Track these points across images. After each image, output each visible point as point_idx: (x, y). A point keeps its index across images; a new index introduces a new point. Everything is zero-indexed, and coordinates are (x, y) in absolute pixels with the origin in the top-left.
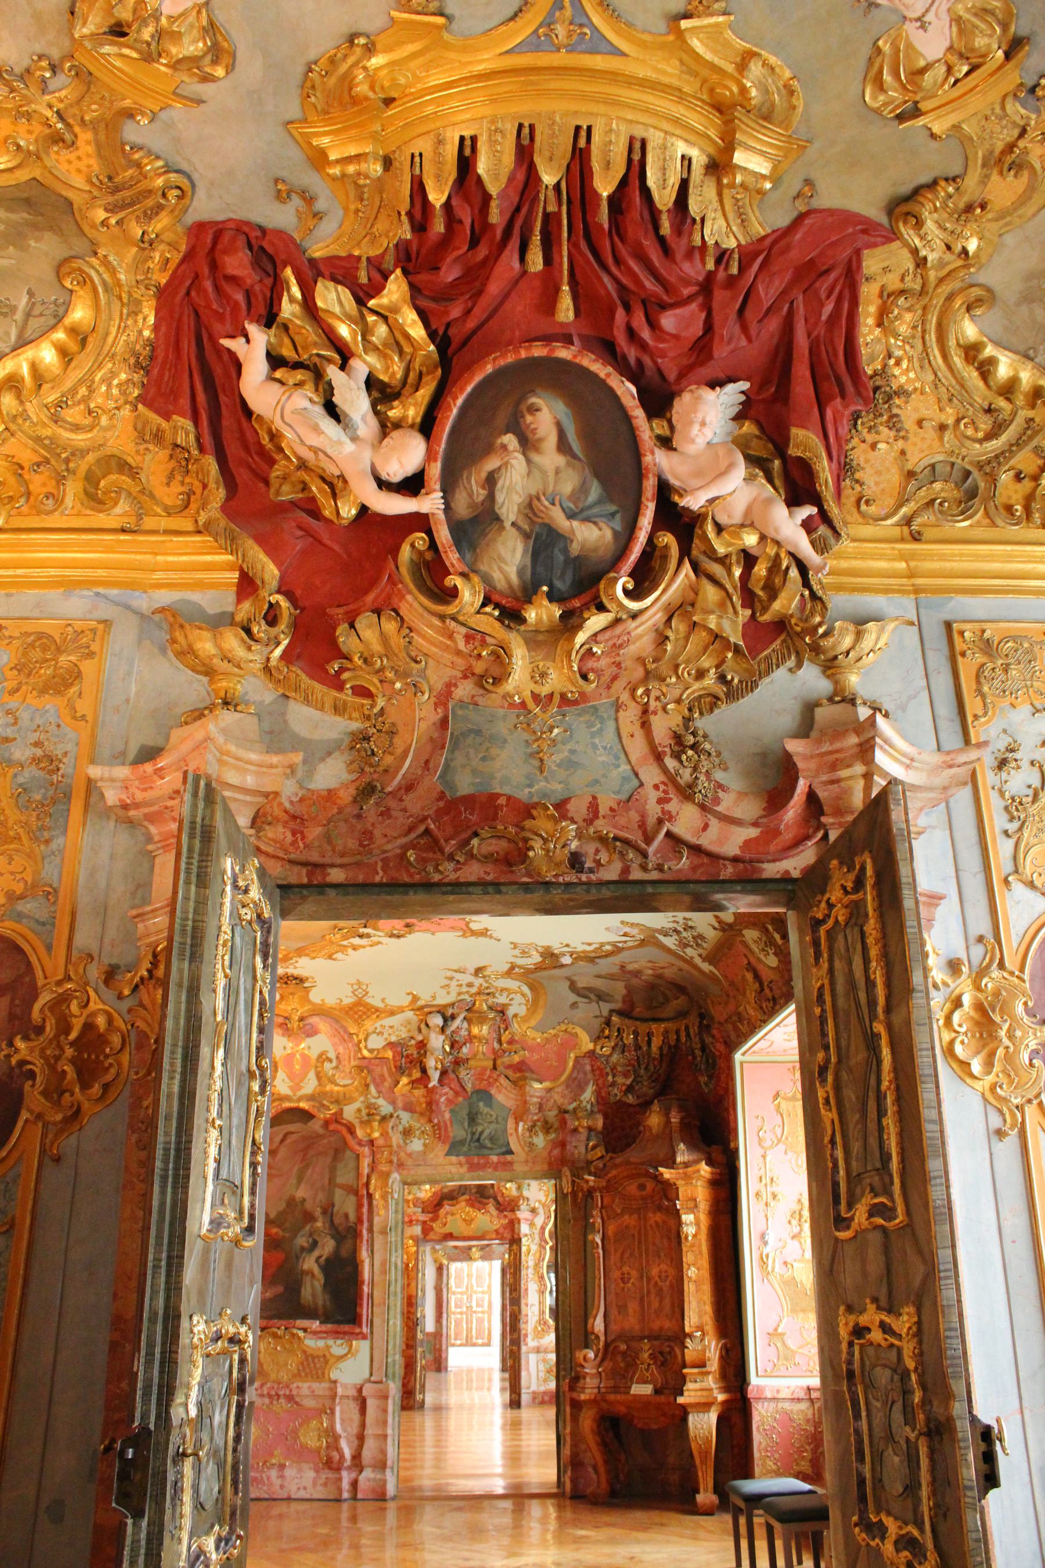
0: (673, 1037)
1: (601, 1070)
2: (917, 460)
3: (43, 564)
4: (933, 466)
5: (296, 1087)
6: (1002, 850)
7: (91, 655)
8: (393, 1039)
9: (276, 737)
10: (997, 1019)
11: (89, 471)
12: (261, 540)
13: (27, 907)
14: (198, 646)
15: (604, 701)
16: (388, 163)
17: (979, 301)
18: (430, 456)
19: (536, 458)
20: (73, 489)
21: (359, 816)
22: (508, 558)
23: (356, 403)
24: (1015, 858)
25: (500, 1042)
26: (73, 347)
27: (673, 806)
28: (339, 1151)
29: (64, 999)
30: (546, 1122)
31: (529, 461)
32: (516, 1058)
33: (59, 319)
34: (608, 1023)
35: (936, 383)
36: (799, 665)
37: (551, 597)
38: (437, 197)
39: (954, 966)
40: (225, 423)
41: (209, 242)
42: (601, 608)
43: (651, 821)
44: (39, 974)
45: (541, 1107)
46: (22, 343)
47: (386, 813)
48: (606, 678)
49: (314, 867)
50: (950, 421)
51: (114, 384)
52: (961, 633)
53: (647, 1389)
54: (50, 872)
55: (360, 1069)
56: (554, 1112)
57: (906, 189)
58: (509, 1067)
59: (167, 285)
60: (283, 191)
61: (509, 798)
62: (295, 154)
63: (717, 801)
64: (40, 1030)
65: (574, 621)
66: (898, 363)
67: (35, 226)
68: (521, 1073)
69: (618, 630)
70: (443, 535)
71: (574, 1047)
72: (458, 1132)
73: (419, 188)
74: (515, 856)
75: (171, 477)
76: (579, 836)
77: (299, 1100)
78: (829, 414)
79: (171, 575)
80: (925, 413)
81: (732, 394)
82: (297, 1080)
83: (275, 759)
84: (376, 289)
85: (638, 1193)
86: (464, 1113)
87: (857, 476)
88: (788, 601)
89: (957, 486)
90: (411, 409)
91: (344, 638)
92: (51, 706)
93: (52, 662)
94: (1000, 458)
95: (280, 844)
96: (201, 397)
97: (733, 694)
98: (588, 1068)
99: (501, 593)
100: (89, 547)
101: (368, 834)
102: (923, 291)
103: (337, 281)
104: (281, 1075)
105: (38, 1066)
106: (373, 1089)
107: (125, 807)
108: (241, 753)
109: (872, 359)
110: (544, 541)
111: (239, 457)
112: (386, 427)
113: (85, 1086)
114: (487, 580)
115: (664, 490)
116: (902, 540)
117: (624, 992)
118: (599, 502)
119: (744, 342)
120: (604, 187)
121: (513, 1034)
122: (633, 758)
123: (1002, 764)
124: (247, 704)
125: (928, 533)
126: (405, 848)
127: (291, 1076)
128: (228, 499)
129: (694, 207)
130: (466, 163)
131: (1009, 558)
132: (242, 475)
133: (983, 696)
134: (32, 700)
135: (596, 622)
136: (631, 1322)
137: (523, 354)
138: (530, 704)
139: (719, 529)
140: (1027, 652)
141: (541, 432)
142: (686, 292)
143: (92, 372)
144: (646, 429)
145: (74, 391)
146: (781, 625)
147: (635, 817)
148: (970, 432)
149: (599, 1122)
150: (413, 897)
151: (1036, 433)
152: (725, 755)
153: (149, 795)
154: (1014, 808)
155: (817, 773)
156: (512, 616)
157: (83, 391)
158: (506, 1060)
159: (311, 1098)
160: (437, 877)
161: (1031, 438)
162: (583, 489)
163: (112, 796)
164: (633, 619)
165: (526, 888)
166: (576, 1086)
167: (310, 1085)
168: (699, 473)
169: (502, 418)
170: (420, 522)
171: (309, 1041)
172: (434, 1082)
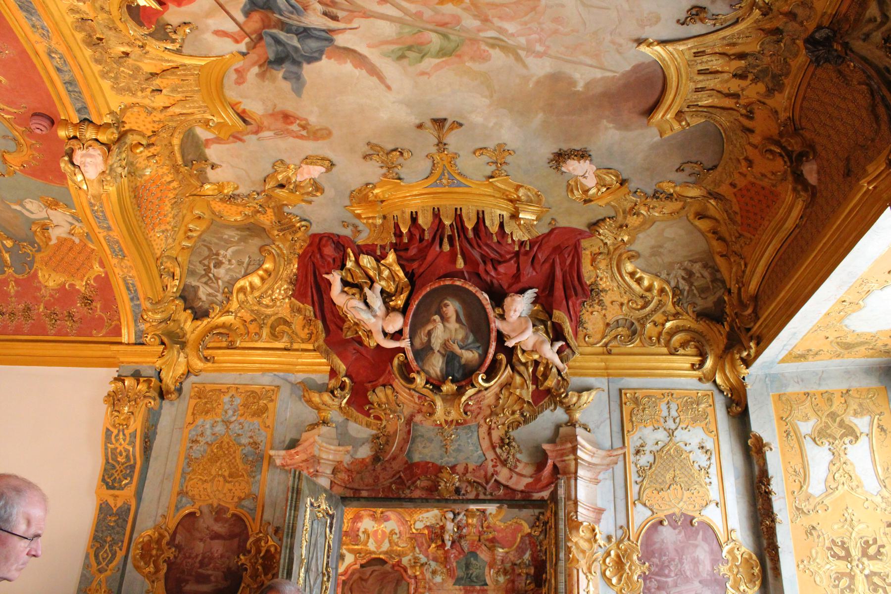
2: (610, 319)
3: (254, 362)
4: (617, 321)
5: (379, 547)
6: (634, 490)
7: (272, 401)
8: (428, 524)
9: (343, 439)
10: (624, 561)
11: (272, 324)
12: (340, 355)
13: (246, 503)
14: (313, 399)
15: (473, 423)
16: (385, 217)
17: (633, 256)
18: (405, 324)
19: (447, 325)
20: (265, 332)
21: (374, 470)
22: (436, 365)
23: (377, 302)
24: (639, 493)
25: (482, 527)
26: (265, 276)
27: (498, 469)
28: (399, 581)
29: (258, 540)
30: (505, 569)
31: (444, 326)
32: (491, 536)
33: (261, 266)
35: (619, 287)
36: (555, 409)
37: (453, 381)
38: (405, 230)
39: (609, 538)
40: (325, 305)
41: (318, 241)
42: (473, 386)
43: (489, 474)
44: (250, 530)
45: (503, 562)
46: (246, 275)
47: (384, 469)
48: (475, 414)
49: (356, 490)
50: (626, 302)
51: (281, 290)
52: (626, 394)
54: (254, 489)
55: (411, 539)
56: (510, 564)
57: (594, 220)
58: (487, 540)
59: (303, 253)
60: (345, 224)
61: (433, 464)
62: (349, 215)
63: (516, 467)
64: (249, 552)
65: (462, 390)
66: (601, 279)
67: (251, 236)
68: (493, 543)
69: (480, 395)
70: (410, 356)
71: (520, 531)
72: (460, 573)
73: (397, 226)
74: (433, 488)
75: (304, 327)
76: (460, 480)
77: (380, 554)
78: (570, 303)
79: (304, 367)
80: (615, 299)
81: (530, 294)
82: (379, 543)
83: (341, 448)
84: (384, 256)
86: (463, 563)
87: (585, 326)
88: (551, 383)
89: (628, 329)
90: (400, 302)
91: (371, 397)
92: (256, 421)
93: (256, 403)
94: (646, 317)
95: (343, 480)
96: (316, 298)
97: (526, 421)
98: (527, 542)
99: (433, 379)
100: (271, 356)
101: (377, 477)
102: (608, 253)
103: (368, 254)
104: (371, 540)
105: (248, 565)
106: (417, 549)
107: (283, 466)
108: (328, 446)
109: (590, 278)
110: (451, 358)
111: (331, 320)
112: (389, 310)
113: (266, 574)
114: (427, 373)
115: (501, 337)
116: (603, 354)
118: (473, 342)
119: (534, 273)
120: (470, 226)
121: (489, 523)
122: (484, 448)
123: (638, 452)
124: (333, 422)
125: (614, 351)
126: (391, 483)
127: (376, 541)
128: (327, 336)
129: (507, 230)
130: (414, 219)
131: (649, 361)
132: (332, 327)
133: (632, 422)
134: (249, 419)
135: (471, 392)
137: (442, 283)
138: (444, 424)
139: (524, 351)
140: (654, 402)
141: (449, 315)
142: (508, 257)
143: (273, 285)
144: (491, 314)
145: (266, 292)
146: (548, 391)
147: (483, 472)
148: (634, 306)
149: (532, 571)
150: (393, 503)
151: (663, 306)
152: (521, 447)
153: (293, 461)
154: (641, 472)
155: (556, 457)
156: (437, 388)
157: (270, 292)
158: (485, 536)
159: (386, 553)
160: (403, 496)
161: (661, 308)
162: (466, 337)
163: (278, 462)
164: (485, 389)
165: (438, 501)
166: (521, 551)
167: (386, 546)
168: (514, 330)
169: (434, 308)
170: (401, 350)
171: (386, 524)
172: (448, 547)
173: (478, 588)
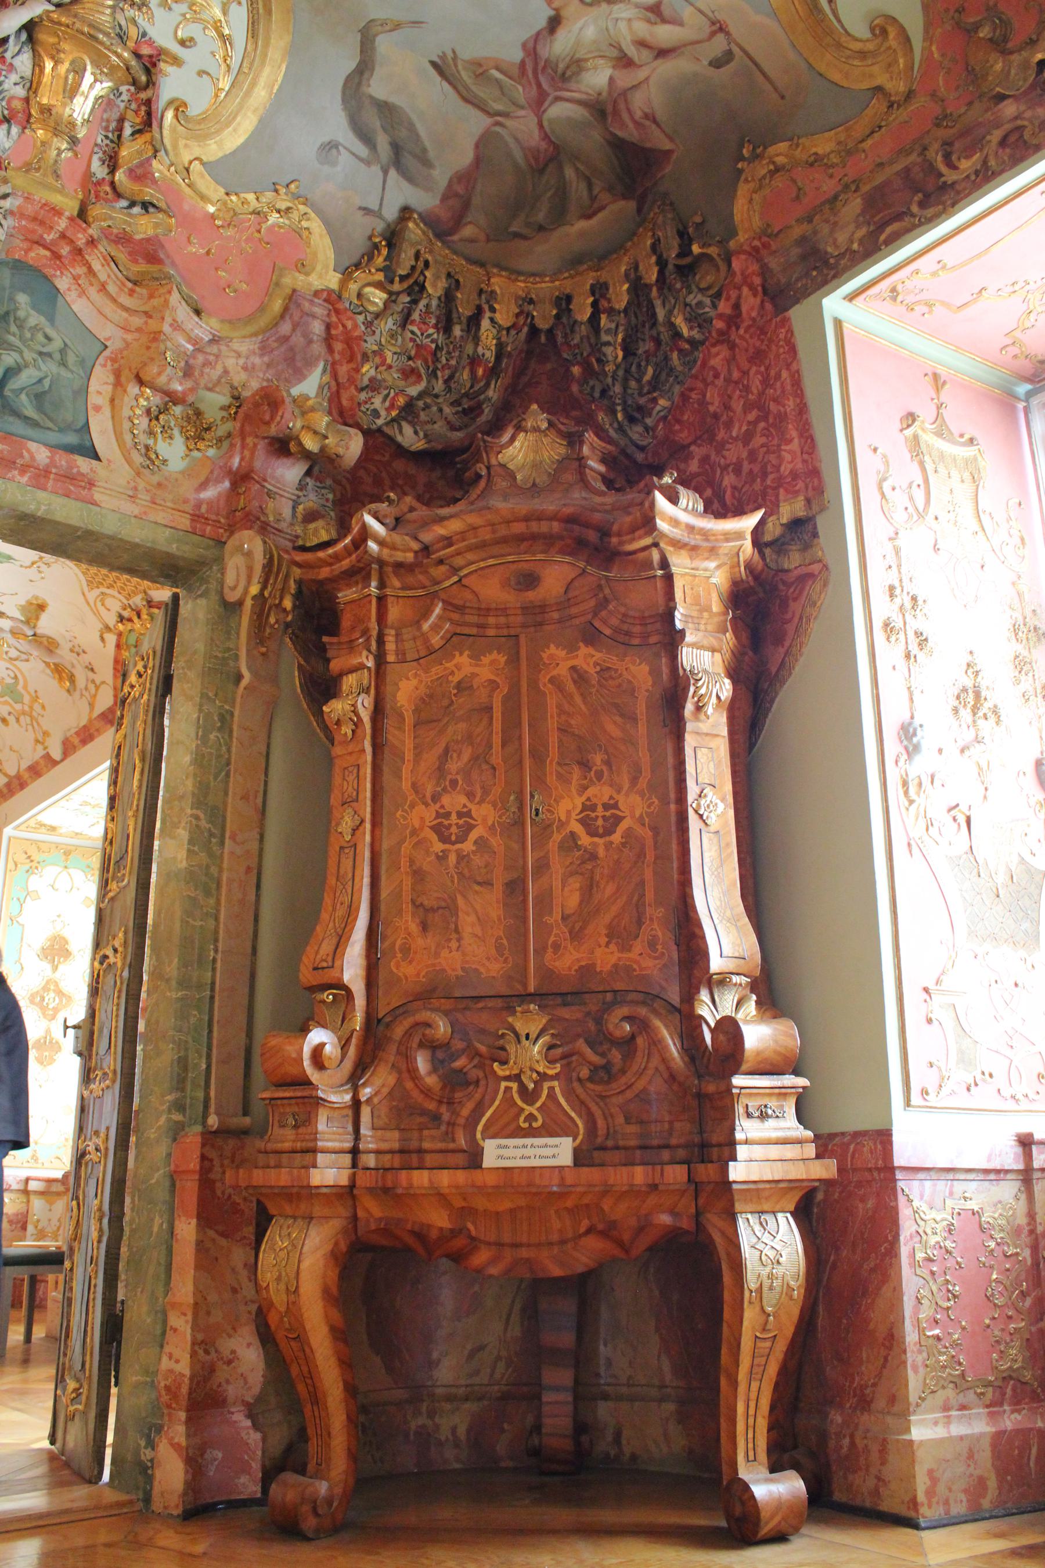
0: (544, 316)
1: (350, 341)
32: (144, 226)
34: (393, 237)
53: (558, 1152)
85: (510, 598)
98: (317, 328)
117: (467, 158)
136: (474, 949)
173: (42, 455)
